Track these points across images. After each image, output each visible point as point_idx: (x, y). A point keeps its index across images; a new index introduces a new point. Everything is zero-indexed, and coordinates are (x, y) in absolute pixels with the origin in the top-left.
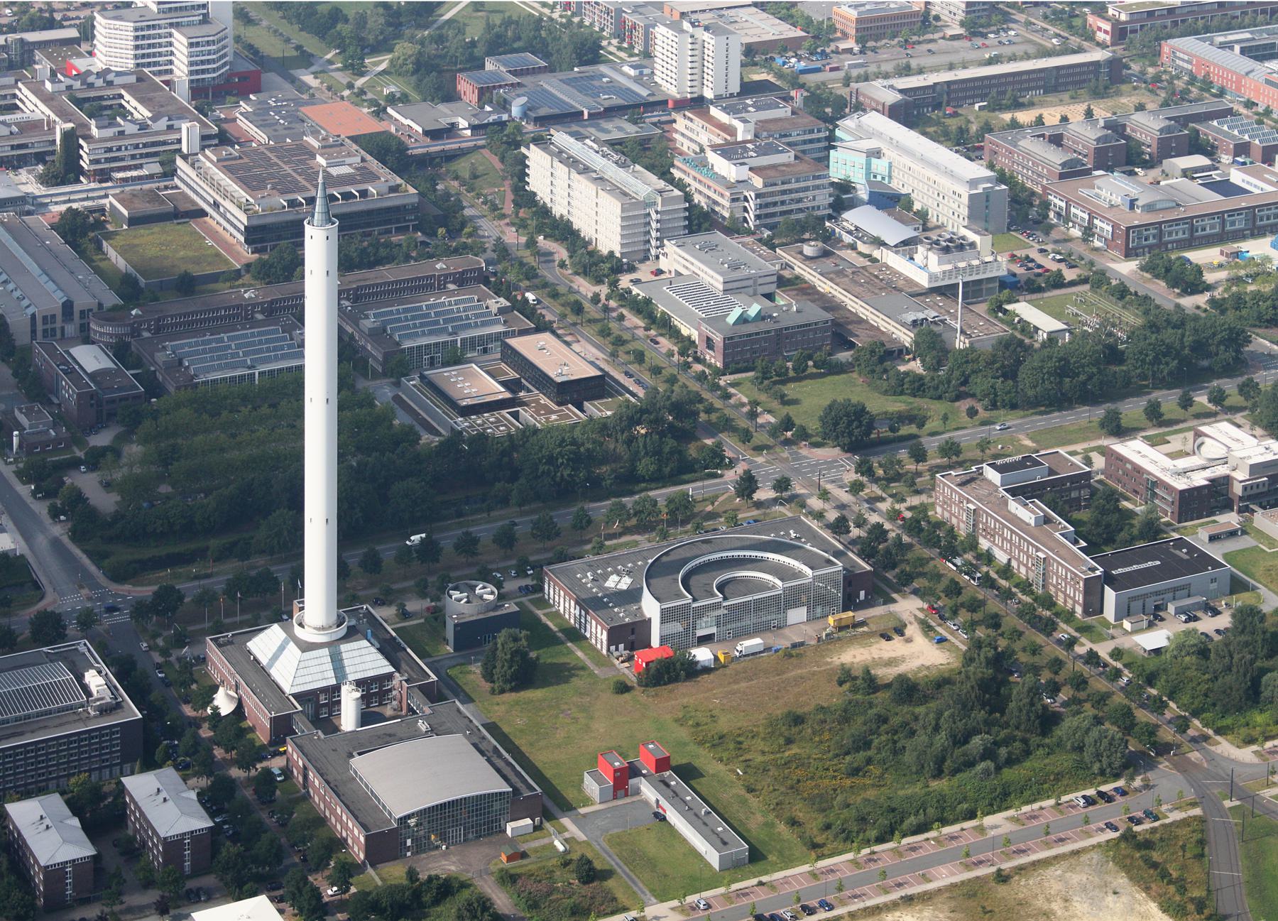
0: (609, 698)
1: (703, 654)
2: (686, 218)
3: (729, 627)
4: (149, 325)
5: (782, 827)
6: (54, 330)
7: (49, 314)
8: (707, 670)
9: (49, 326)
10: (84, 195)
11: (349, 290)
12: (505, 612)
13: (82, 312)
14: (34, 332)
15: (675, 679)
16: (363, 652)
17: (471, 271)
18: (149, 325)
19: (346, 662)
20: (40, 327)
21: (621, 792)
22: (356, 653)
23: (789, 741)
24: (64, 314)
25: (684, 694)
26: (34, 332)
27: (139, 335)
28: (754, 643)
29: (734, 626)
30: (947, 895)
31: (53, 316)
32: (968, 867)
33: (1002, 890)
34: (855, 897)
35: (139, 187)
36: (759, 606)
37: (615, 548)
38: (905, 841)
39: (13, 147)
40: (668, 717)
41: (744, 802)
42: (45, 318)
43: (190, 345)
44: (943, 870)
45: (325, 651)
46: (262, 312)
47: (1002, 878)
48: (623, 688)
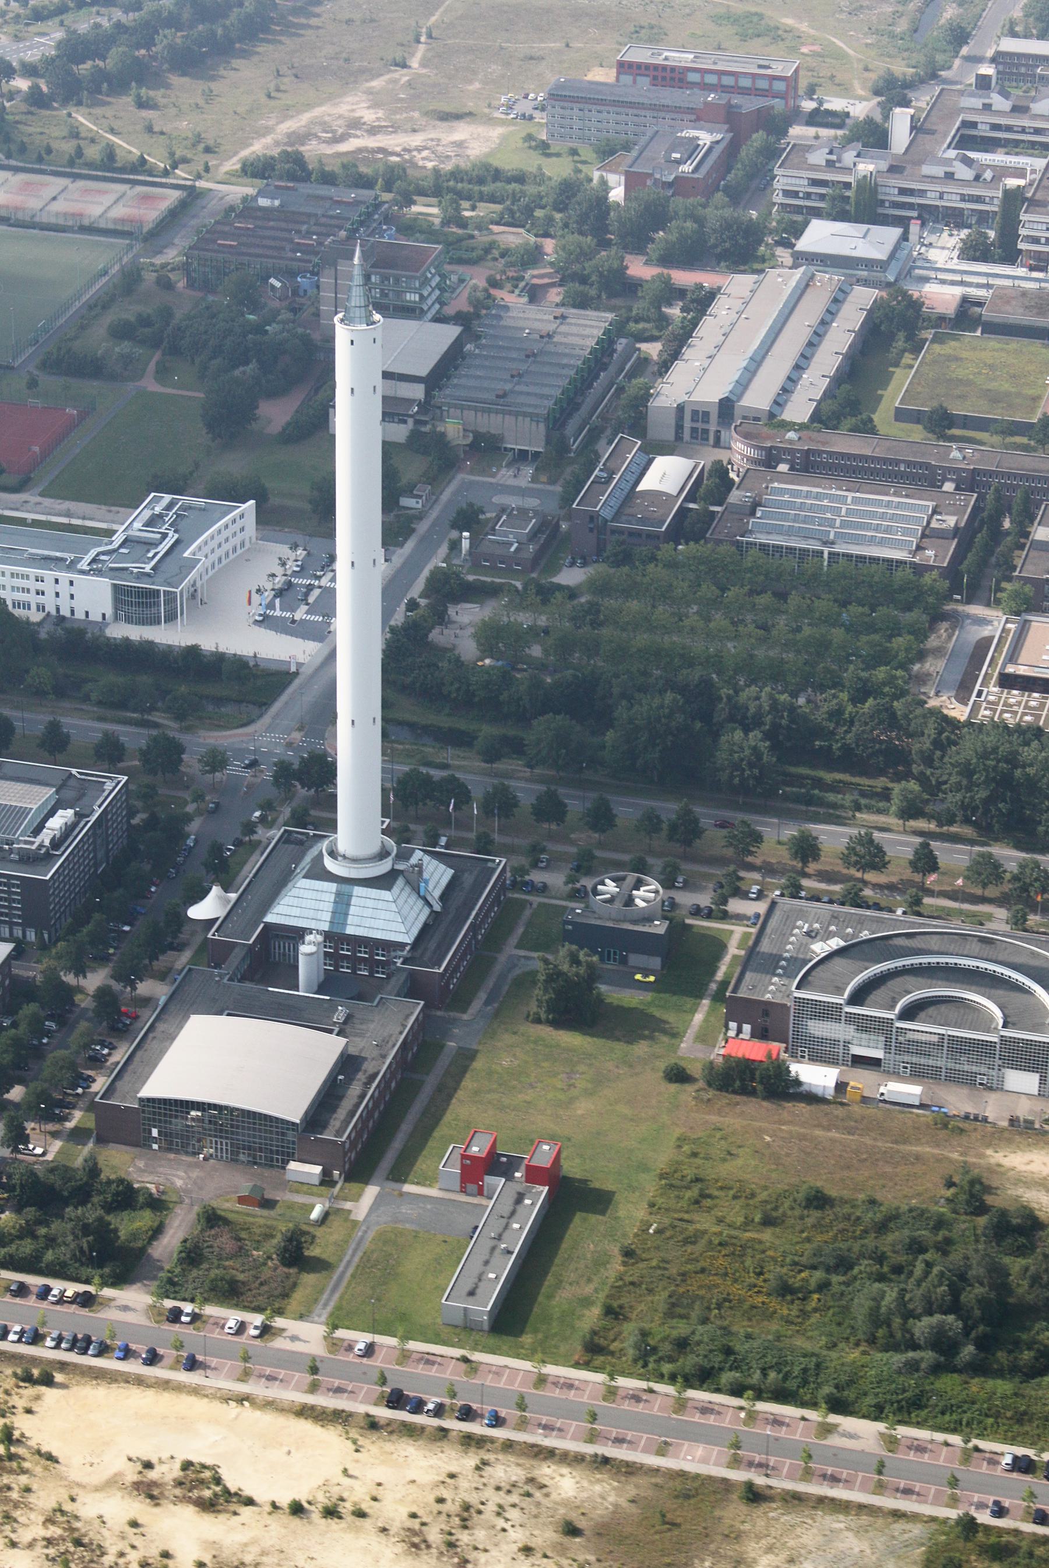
0: (652, 1079)
1: (817, 1077)
3: (906, 1058)
5: (596, 1311)
6: (706, 431)
7: (701, 409)
8: (812, 1098)
9: (699, 425)
10: (958, 278)
12: (650, 930)
14: (679, 427)
15: (747, 1091)
16: (380, 905)
19: (352, 910)
20: (688, 424)
21: (472, 1187)
22: (370, 903)
23: (768, 1222)
24: (721, 415)
25: (749, 1117)
26: (679, 427)
28: (910, 1091)
29: (915, 1060)
30: (659, 1480)
31: (706, 414)
32: (735, 1462)
33: (735, 1512)
34: (545, 1427)
36: (958, 1047)
37: (943, 915)
38: (762, 1406)
39: (963, 198)
40: (678, 1132)
41: (601, 1262)
44: (700, 1450)
45: (333, 887)
47: (754, 1496)
48: (678, 1076)
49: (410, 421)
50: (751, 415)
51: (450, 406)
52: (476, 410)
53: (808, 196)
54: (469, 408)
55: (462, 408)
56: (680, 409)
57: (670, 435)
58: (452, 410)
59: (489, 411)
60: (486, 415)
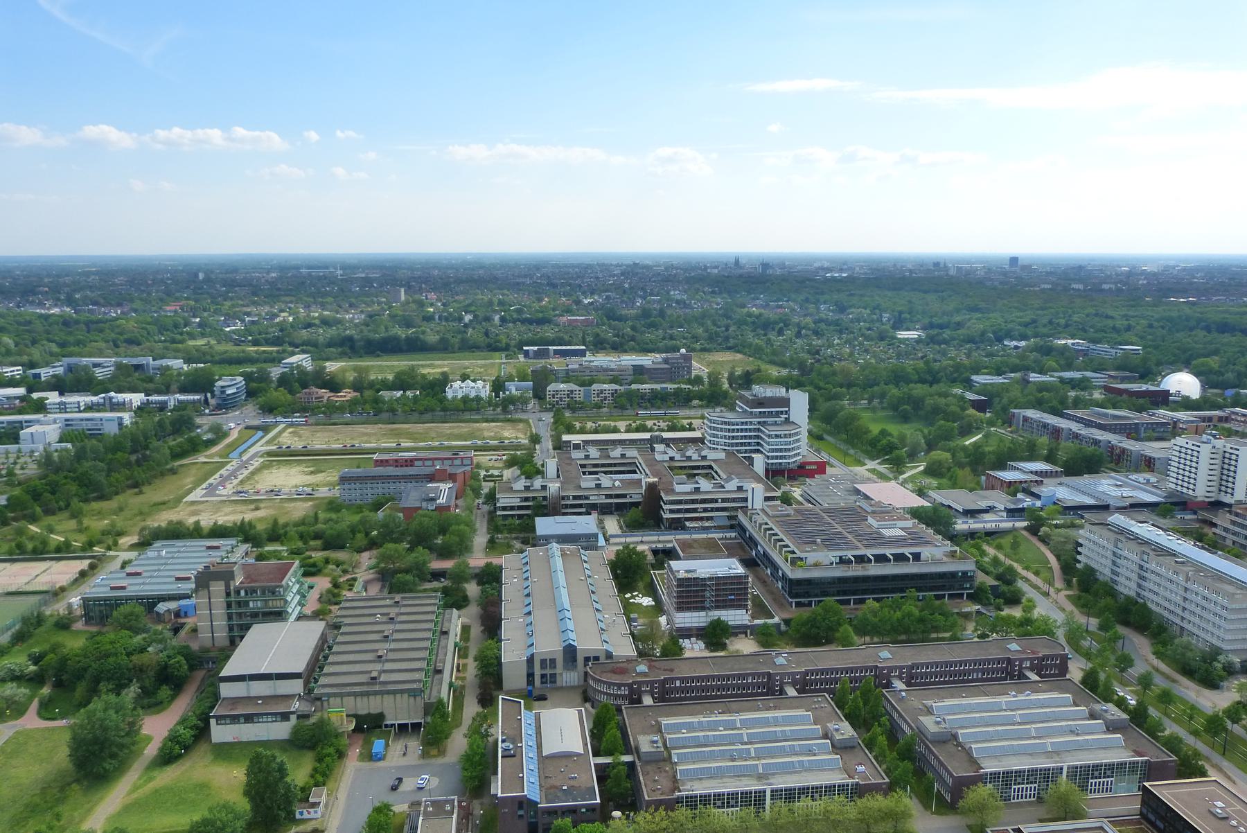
4: (652, 688)
9: (548, 671)
11: (903, 667)
13: (587, 659)
14: (530, 676)
17: (1052, 657)
18: (652, 688)
20: (538, 672)
24: (565, 660)
27: (639, 701)
31: (553, 661)
35: (704, 536)
42: (543, 662)
43: (690, 727)
46: (794, 684)
49: (293, 718)
50: (592, 656)
51: (329, 695)
52: (355, 694)
53: (520, 508)
54: (349, 694)
55: (341, 695)
56: (530, 661)
57: (522, 683)
58: (332, 700)
59: (367, 694)
60: (365, 699)
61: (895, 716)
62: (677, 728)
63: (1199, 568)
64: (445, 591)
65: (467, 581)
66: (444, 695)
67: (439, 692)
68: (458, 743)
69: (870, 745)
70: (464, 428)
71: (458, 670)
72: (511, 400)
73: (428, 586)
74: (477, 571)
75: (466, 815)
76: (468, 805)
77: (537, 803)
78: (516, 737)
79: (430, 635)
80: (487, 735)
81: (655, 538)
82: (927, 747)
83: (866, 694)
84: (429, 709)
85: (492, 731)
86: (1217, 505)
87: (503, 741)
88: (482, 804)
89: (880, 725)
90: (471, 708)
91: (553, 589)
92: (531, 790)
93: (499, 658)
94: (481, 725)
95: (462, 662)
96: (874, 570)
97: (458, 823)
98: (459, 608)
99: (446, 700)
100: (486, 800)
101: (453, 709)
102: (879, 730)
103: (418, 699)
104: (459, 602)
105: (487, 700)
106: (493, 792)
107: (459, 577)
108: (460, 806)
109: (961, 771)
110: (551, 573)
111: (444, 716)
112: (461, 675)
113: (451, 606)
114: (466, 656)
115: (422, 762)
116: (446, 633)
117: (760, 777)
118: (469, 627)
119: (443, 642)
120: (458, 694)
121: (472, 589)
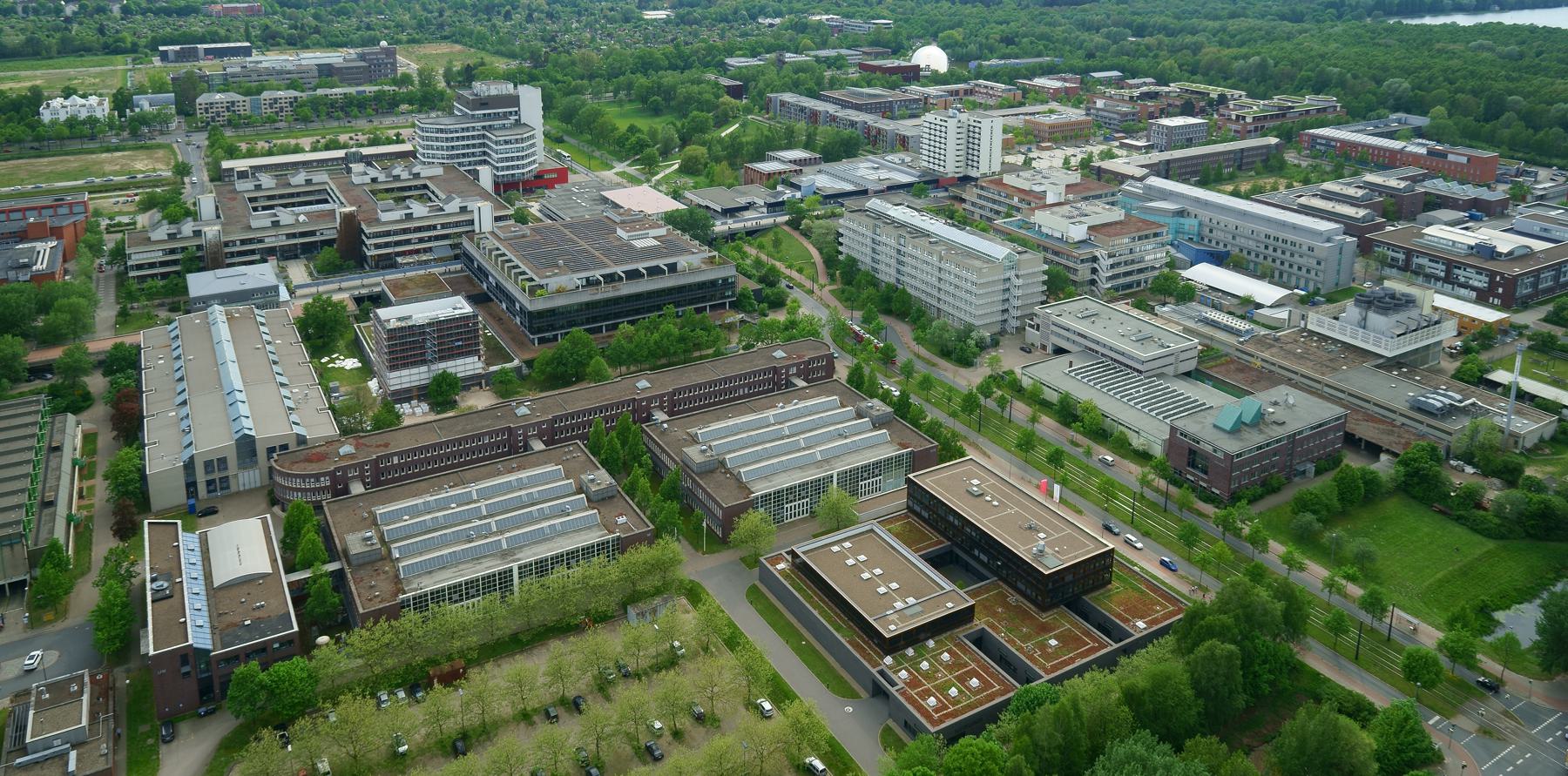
2: (1044, 283)
4: (362, 471)
7: (214, 457)
9: (216, 475)
11: (663, 395)
13: (271, 450)
14: (191, 486)
18: (362, 471)
20: (201, 478)
27: (346, 491)
31: (223, 462)
35: (422, 272)
43: (414, 512)
46: (540, 436)
50: (277, 445)
53: (163, 264)
56: (189, 466)
57: (180, 497)
61: (658, 451)
62: (396, 516)
63: (951, 245)
64: (54, 393)
65: (86, 372)
66: (59, 534)
67: (52, 531)
68: (86, 597)
69: (631, 491)
70: (74, 162)
71: (81, 497)
72: (143, 120)
73: (25, 387)
74: (102, 357)
75: (103, 692)
76: (106, 678)
77: (209, 651)
78: (170, 571)
79: (31, 455)
80: (130, 575)
81: (358, 282)
82: (694, 481)
83: (624, 435)
84: (34, 559)
85: (137, 569)
86: (966, 180)
87: (153, 580)
88: (128, 671)
89: (641, 466)
90: (104, 544)
91: (217, 365)
92: (199, 635)
93: (141, 471)
94: (119, 565)
95: (86, 484)
96: (627, 289)
97: (92, 705)
98: (75, 412)
99: (62, 541)
100: (132, 665)
101: (76, 552)
102: (640, 471)
103: (17, 548)
104: (80, 403)
105: (126, 529)
106: (143, 651)
107: (73, 370)
108: (93, 681)
109: (728, 500)
110: (212, 346)
111: (61, 565)
112: (86, 502)
113: (66, 410)
114: (92, 476)
115: (30, 633)
116: (58, 449)
117: (504, 555)
118: (95, 434)
119: (53, 464)
120: (82, 530)
121: (96, 383)
